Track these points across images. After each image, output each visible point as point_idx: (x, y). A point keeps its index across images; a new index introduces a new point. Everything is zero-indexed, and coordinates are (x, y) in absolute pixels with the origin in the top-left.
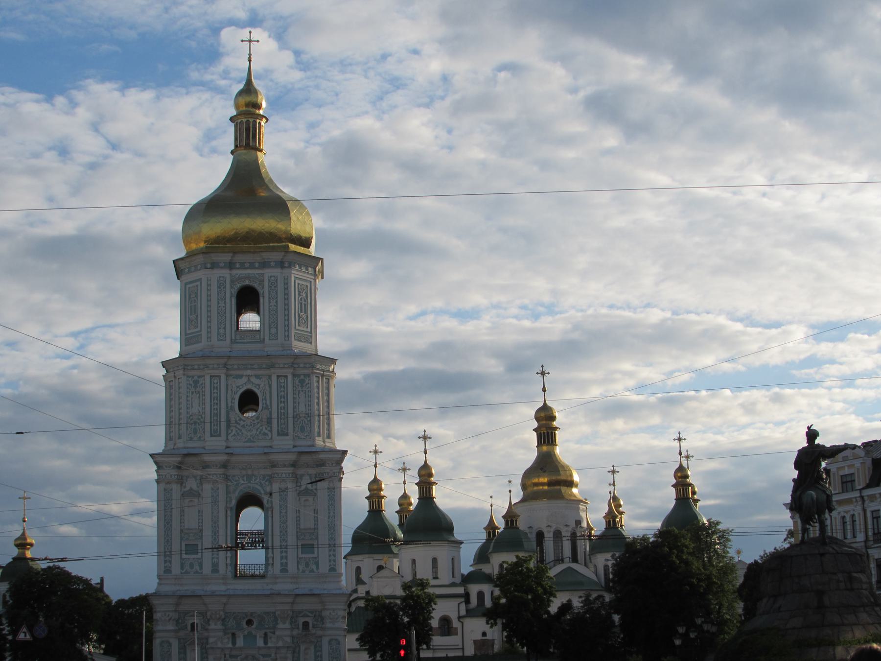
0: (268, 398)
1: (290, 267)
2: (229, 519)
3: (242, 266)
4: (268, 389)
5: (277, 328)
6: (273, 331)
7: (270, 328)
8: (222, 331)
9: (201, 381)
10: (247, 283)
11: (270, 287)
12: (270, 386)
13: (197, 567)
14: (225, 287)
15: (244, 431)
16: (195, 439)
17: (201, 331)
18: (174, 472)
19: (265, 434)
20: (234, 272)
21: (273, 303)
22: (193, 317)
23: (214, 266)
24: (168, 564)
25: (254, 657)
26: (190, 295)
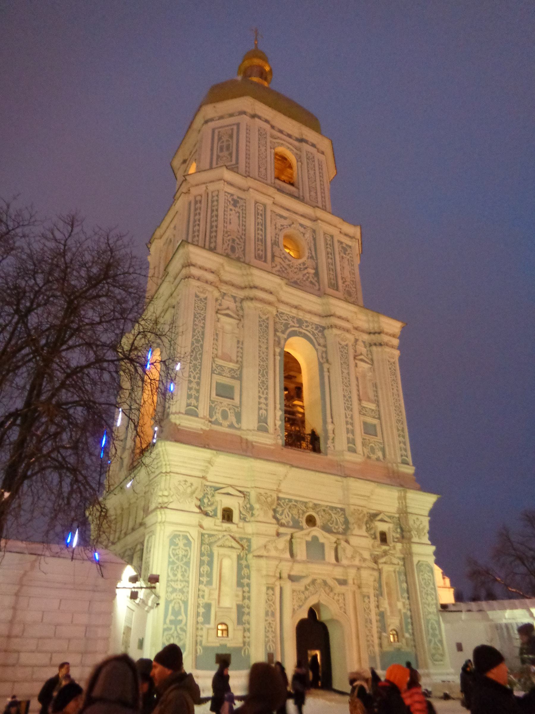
0: (313, 249)
1: (323, 153)
4: (313, 242)
7: (310, 191)
9: (241, 202)
12: (314, 239)
13: (232, 418)
15: (289, 270)
17: (237, 163)
19: (311, 282)
21: (312, 172)
24: (193, 401)
25: (325, 583)
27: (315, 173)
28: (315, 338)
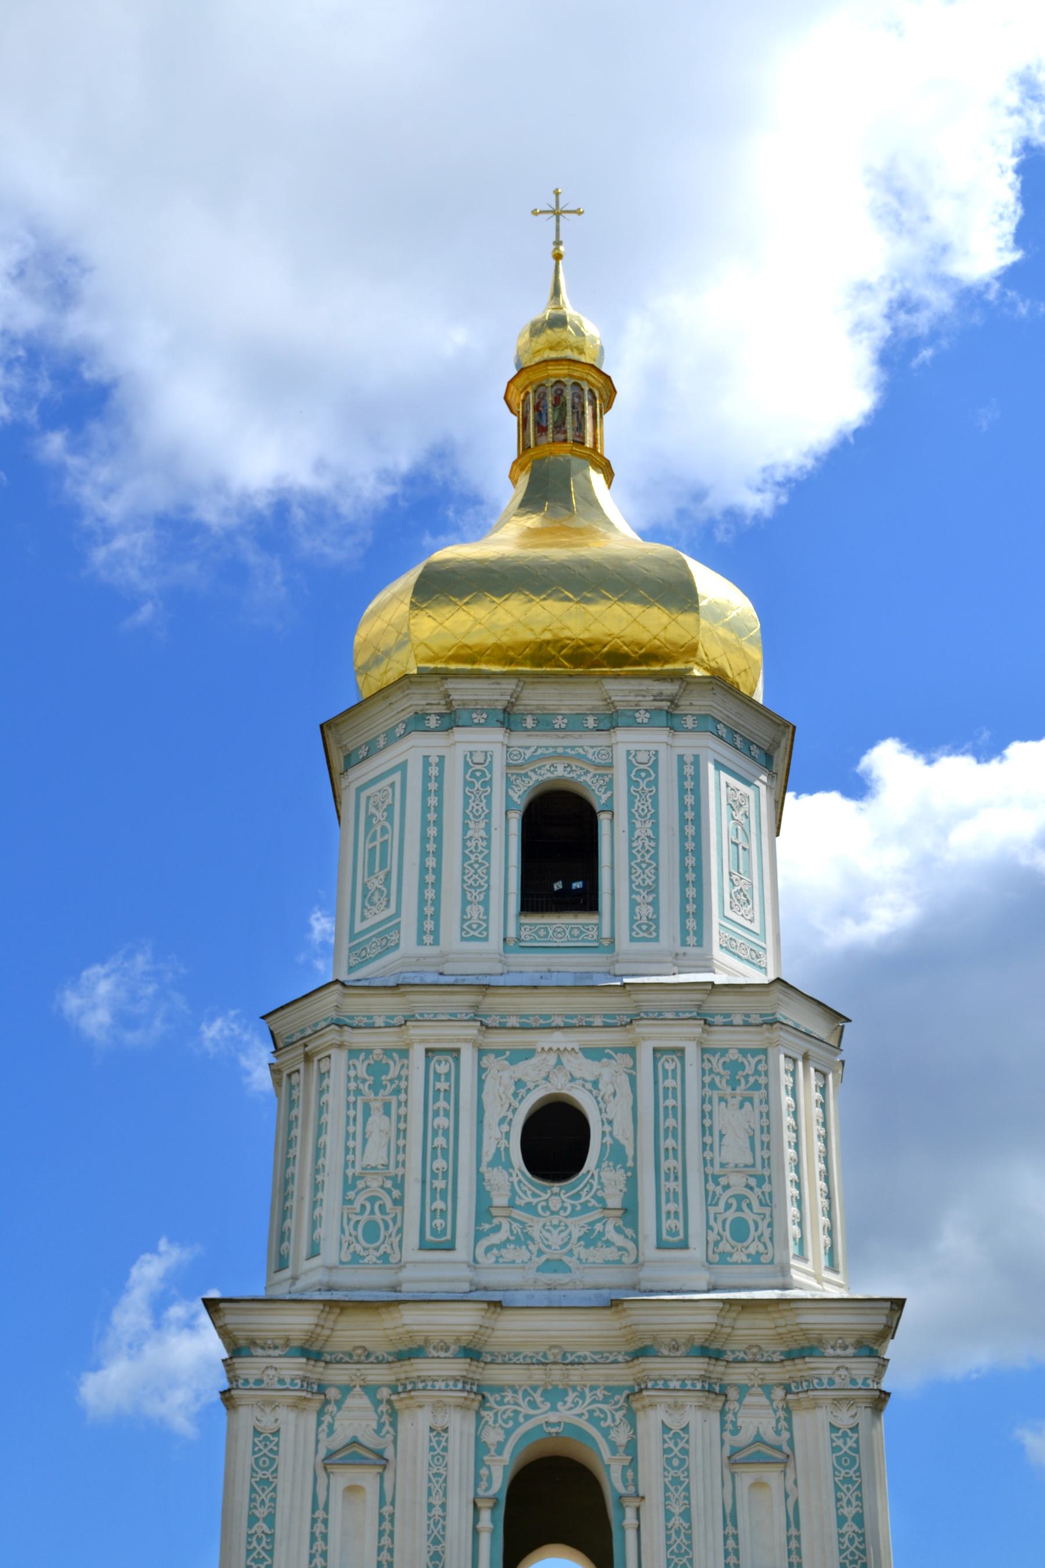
2: (485, 1540)
3: (544, 723)
5: (655, 904)
6: (645, 911)
7: (633, 904)
8: (475, 912)
10: (560, 772)
11: (631, 782)
14: (488, 783)
16: (372, 1257)
18: (292, 1367)
20: (519, 740)
21: (643, 829)
22: (376, 883)
23: (451, 719)
26: (370, 817)
27: (655, 827)
28: (605, 1432)
